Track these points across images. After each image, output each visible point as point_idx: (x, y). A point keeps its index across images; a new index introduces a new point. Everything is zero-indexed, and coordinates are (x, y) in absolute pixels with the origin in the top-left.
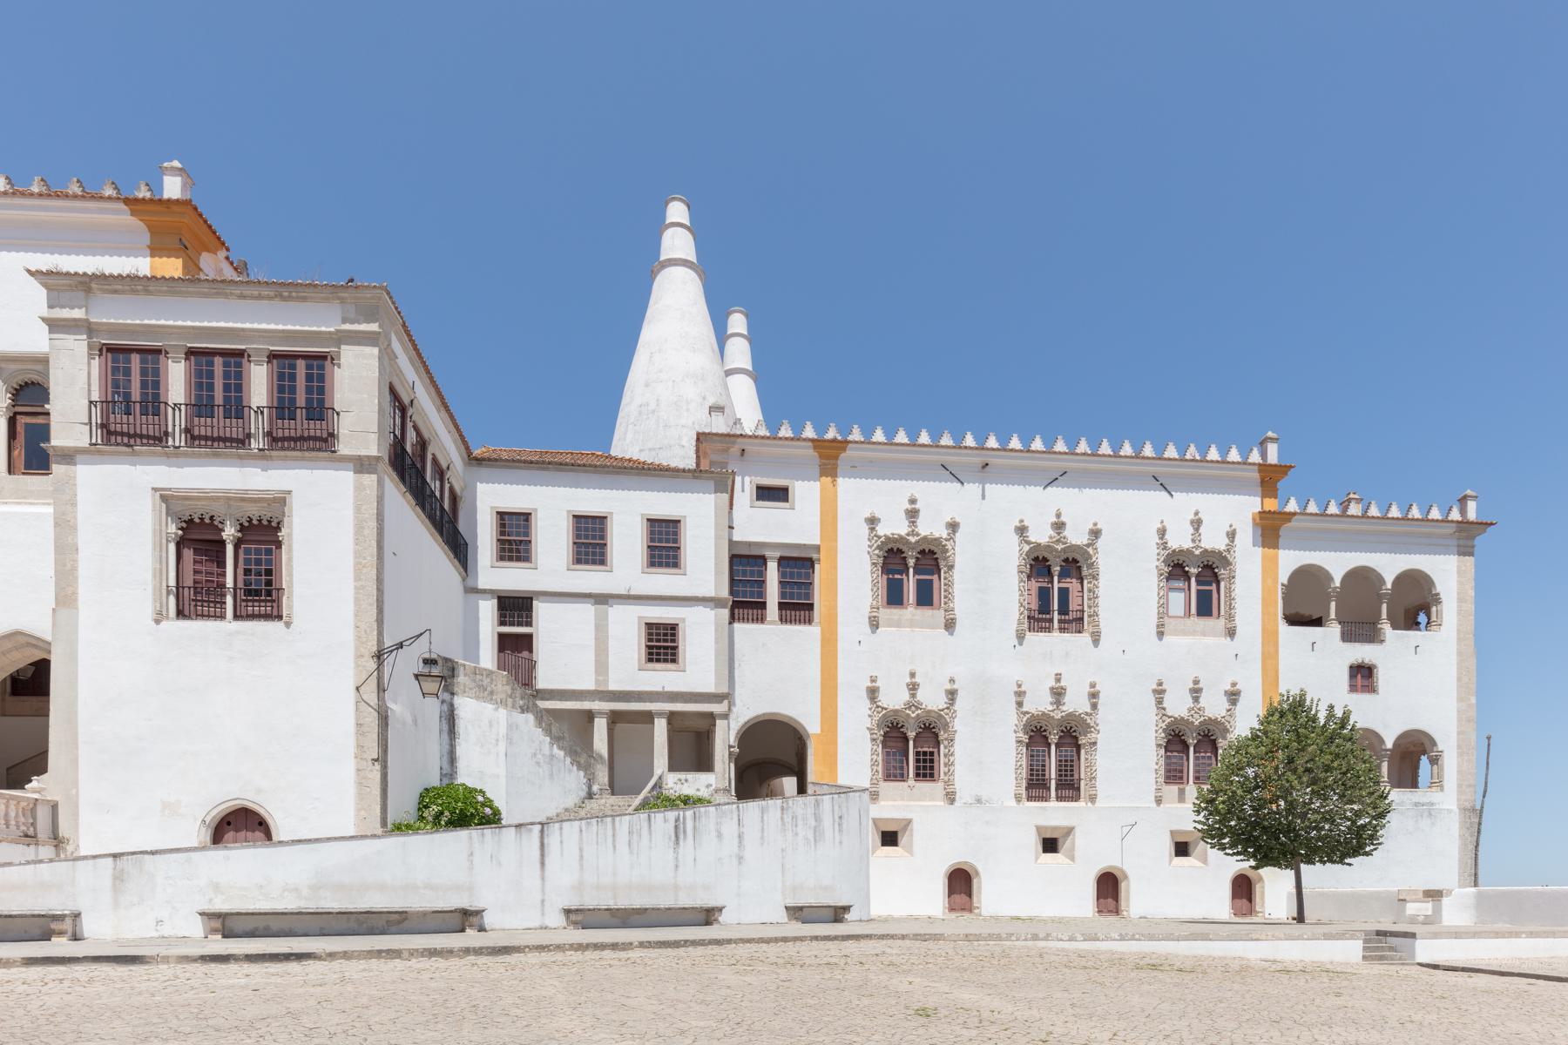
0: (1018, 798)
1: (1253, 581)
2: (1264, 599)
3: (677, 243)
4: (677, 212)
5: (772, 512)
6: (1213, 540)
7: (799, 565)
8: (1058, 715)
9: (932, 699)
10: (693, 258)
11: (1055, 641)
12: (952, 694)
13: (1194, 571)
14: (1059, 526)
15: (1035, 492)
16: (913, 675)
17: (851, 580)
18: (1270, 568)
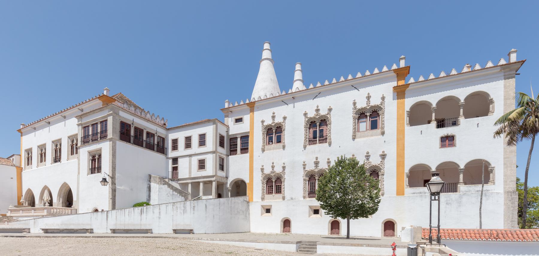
0: (304, 197)
1: (392, 113)
2: (398, 119)
3: (266, 54)
4: (266, 46)
5: (240, 125)
6: (375, 101)
7: (245, 138)
8: (316, 170)
9: (278, 170)
10: (270, 58)
11: (318, 147)
12: (284, 168)
13: (368, 114)
14: (317, 110)
15: (310, 102)
16: (273, 163)
17: (257, 139)
18: (400, 108)
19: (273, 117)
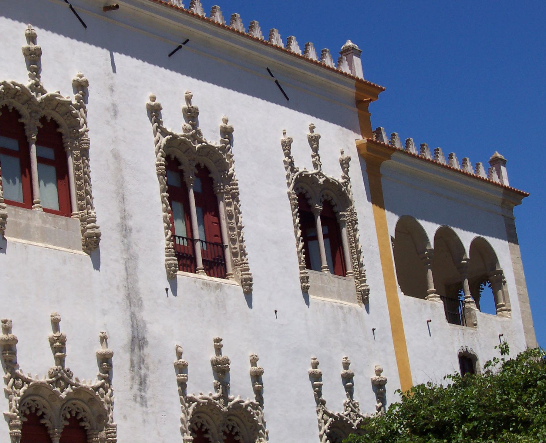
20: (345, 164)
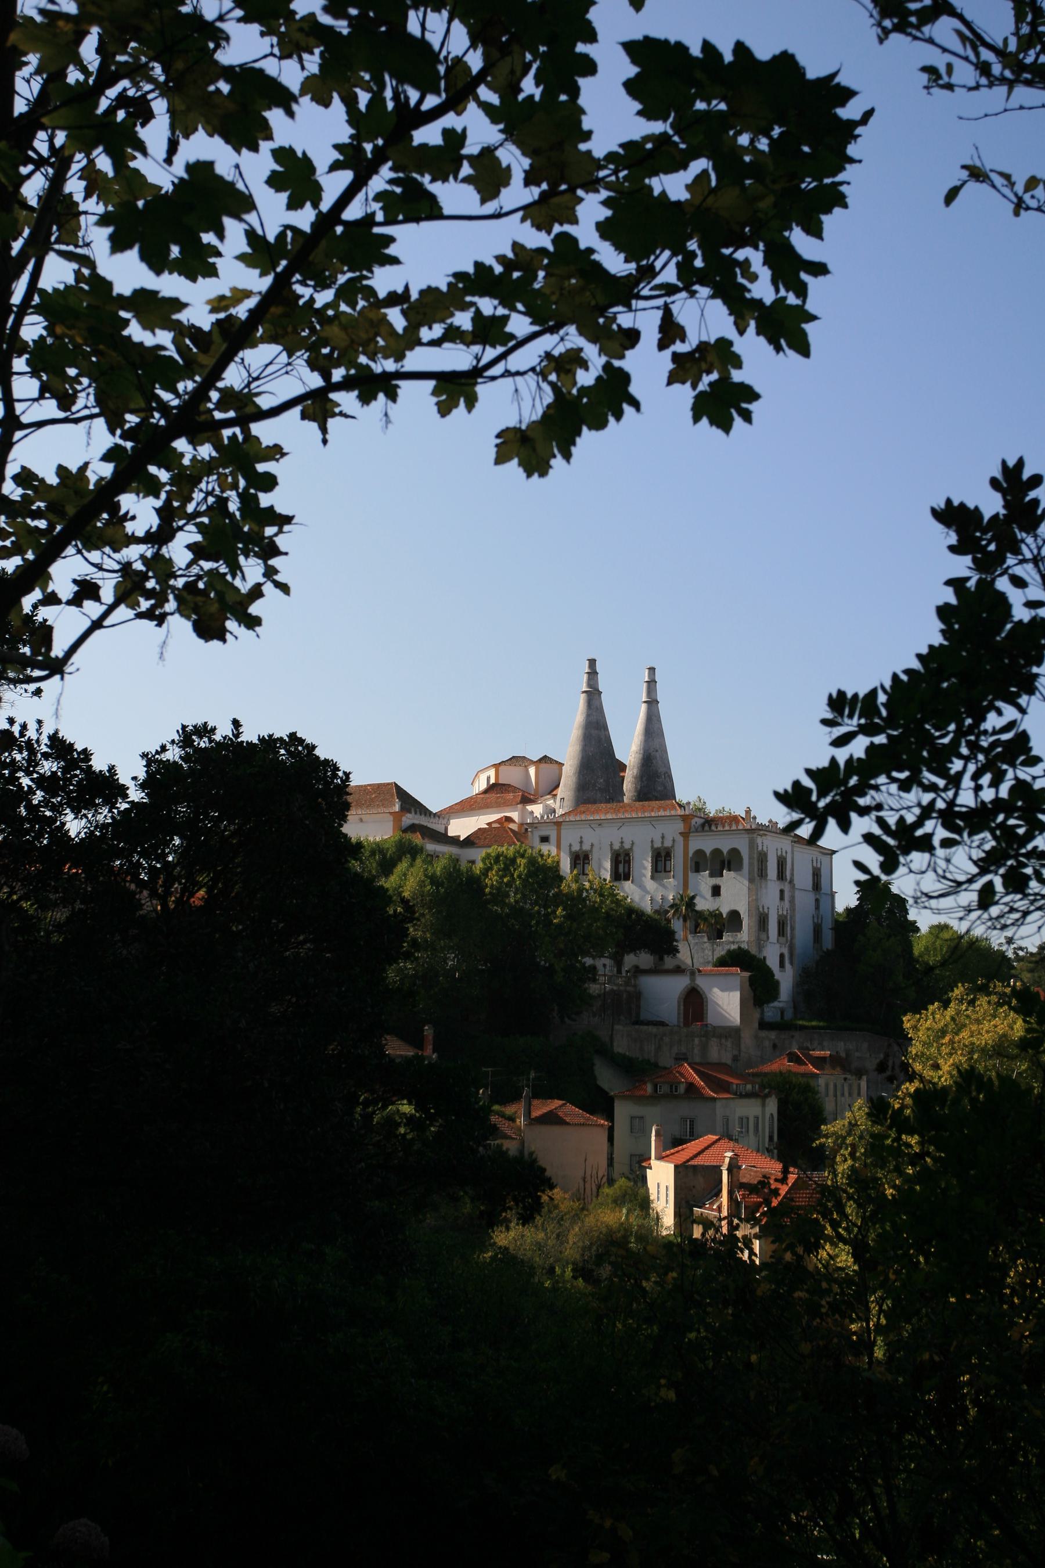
19: (581, 842)
20: (674, 841)
